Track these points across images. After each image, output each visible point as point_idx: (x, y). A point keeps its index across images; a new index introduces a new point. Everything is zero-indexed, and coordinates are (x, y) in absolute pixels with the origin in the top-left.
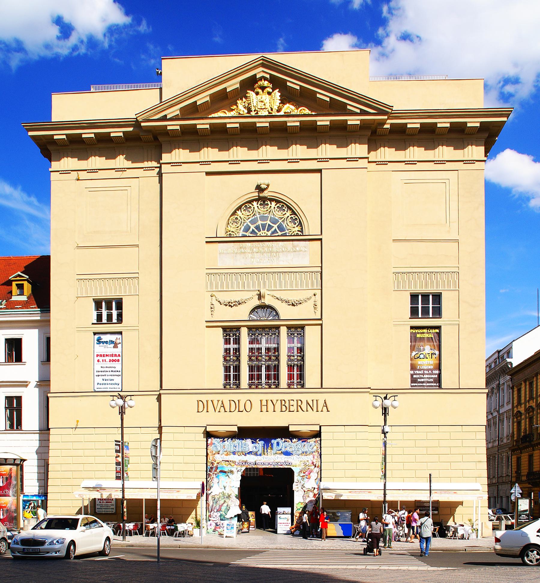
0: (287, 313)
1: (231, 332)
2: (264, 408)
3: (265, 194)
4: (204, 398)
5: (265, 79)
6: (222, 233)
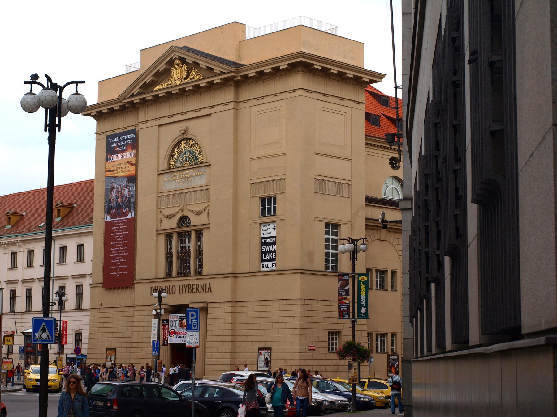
0: (195, 220)
1: (169, 236)
2: (181, 291)
3: (185, 136)
4: (154, 285)
5: (178, 59)
6: (165, 167)
